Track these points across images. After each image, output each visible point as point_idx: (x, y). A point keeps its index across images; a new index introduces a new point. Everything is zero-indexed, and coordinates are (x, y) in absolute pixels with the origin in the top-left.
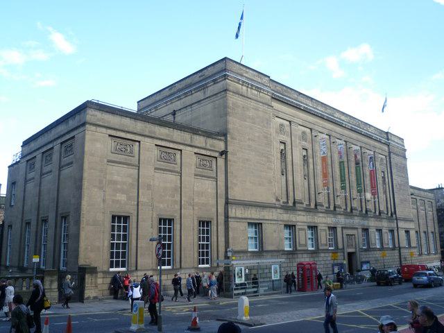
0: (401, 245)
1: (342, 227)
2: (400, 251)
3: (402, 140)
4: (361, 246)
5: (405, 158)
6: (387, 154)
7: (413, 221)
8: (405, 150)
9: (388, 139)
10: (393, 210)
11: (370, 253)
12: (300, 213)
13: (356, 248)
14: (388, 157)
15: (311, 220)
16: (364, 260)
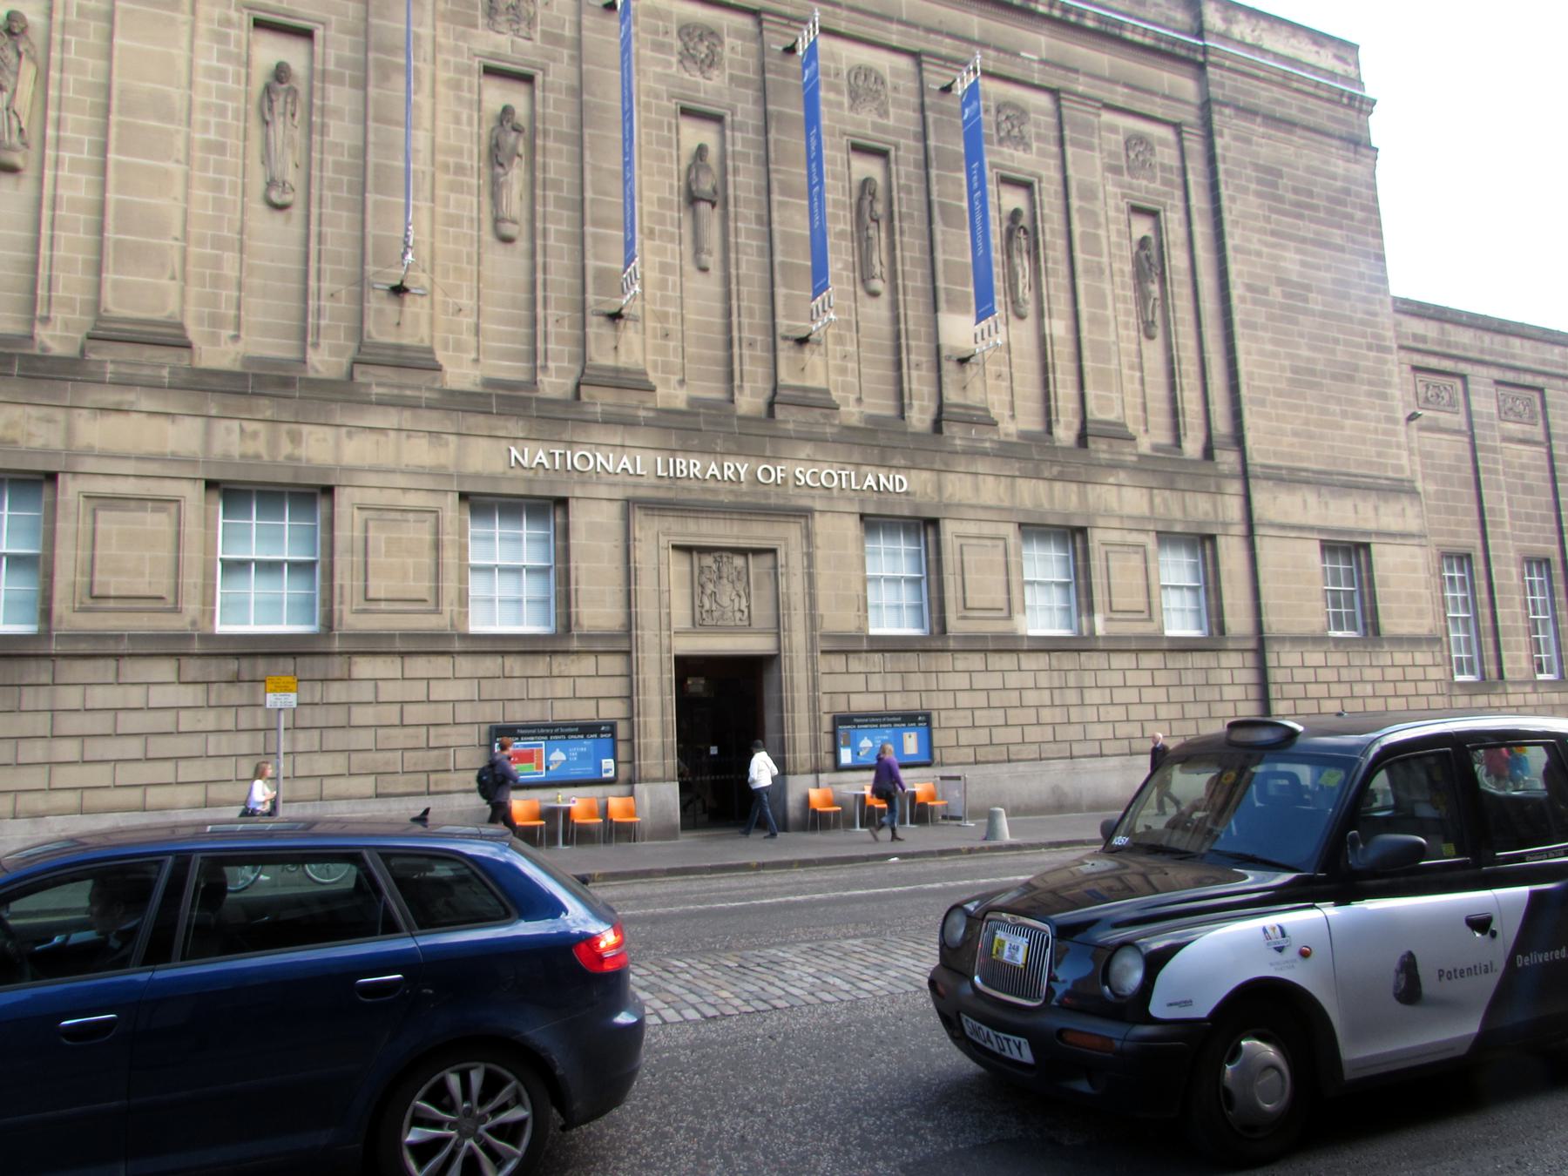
0: (1274, 623)
1: (628, 501)
2: (1260, 651)
3: (1347, 49)
4: (837, 619)
5: (1359, 145)
6: (1189, 116)
7: (1413, 493)
8: (1363, 106)
9: (1200, 33)
10: (1222, 425)
11: (945, 661)
12: (112, 397)
13: (778, 628)
14: (1194, 145)
15: (259, 447)
16: (861, 703)
